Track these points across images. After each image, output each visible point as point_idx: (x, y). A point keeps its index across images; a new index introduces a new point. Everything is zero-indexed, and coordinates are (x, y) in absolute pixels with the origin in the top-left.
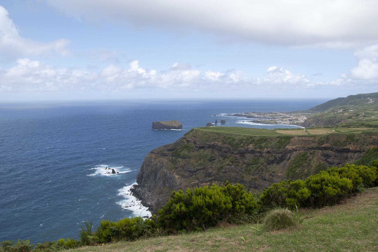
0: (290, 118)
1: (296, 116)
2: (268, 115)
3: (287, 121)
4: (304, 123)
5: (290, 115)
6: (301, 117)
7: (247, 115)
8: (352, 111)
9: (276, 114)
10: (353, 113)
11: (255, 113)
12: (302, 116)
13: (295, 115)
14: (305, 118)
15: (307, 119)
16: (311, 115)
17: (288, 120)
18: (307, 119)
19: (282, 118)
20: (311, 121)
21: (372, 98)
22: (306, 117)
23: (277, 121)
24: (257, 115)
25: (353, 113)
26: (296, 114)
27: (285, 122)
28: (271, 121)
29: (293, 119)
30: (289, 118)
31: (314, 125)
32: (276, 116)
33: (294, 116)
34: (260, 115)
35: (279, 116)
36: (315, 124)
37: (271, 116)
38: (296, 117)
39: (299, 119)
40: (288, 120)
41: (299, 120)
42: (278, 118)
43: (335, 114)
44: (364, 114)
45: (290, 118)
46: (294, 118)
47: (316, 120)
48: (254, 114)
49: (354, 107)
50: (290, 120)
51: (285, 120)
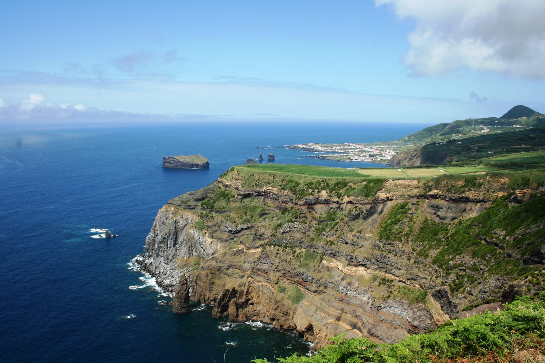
0: (370, 152)
1: (378, 150)
2: (339, 147)
3: (366, 156)
5: (371, 148)
6: (386, 151)
7: (307, 147)
8: (460, 143)
9: (349, 146)
10: (461, 147)
12: (388, 150)
13: (378, 148)
14: (393, 153)
16: (401, 149)
17: (368, 155)
18: (395, 154)
19: (359, 151)
20: (402, 157)
21: (487, 125)
22: (394, 152)
24: (321, 147)
25: (461, 147)
26: (379, 147)
27: (364, 158)
28: (342, 156)
30: (369, 153)
31: (406, 164)
32: (350, 149)
33: (377, 150)
35: (354, 149)
36: (408, 162)
38: (379, 151)
39: (384, 154)
40: (368, 155)
41: (384, 155)
43: (437, 147)
44: (477, 148)
45: (370, 152)
46: (376, 153)
47: (410, 155)
48: (317, 146)
49: (462, 137)
50: (370, 156)
51: (363, 155)
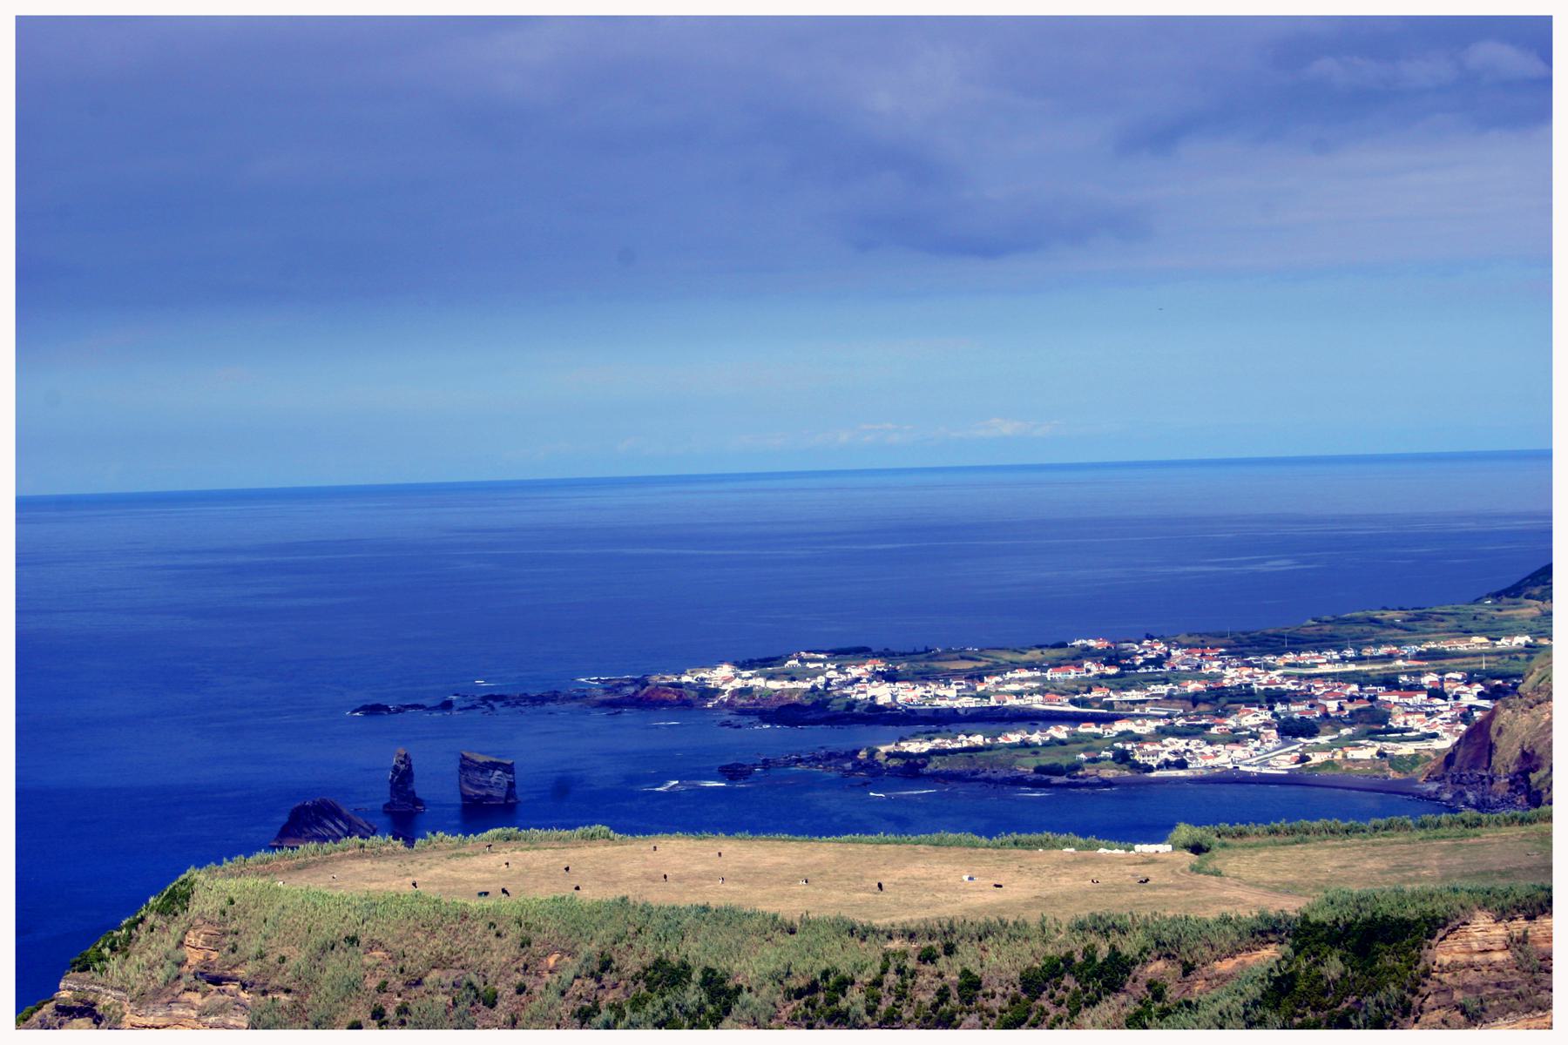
7: (774, 685)
11: (860, 653)
19: (1195, 699)
23: (1138, 739)
29: (1326, 715)
34: (923, 677)
38: (1355, 687)
42: (1148, 710)
46: (1332, 706)
48: (855, 672)
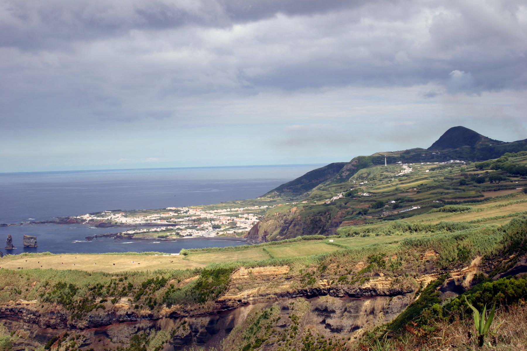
4: (251, 233)
7: (99, 218)
12: (245, 216)
15: (258, 221)
18: (258, 221)
19: (194, 221)
23: (181, 230)
29: (223, 224)
37: (162, 219)
38: (229, 218)
42: (184, 223)
44: (394, 202)
46: (224, 222)
47: (282, 221)
48: (117, 215)
